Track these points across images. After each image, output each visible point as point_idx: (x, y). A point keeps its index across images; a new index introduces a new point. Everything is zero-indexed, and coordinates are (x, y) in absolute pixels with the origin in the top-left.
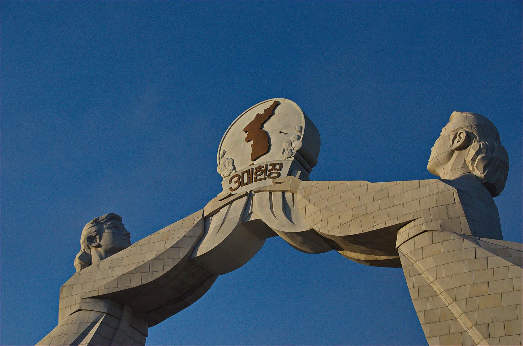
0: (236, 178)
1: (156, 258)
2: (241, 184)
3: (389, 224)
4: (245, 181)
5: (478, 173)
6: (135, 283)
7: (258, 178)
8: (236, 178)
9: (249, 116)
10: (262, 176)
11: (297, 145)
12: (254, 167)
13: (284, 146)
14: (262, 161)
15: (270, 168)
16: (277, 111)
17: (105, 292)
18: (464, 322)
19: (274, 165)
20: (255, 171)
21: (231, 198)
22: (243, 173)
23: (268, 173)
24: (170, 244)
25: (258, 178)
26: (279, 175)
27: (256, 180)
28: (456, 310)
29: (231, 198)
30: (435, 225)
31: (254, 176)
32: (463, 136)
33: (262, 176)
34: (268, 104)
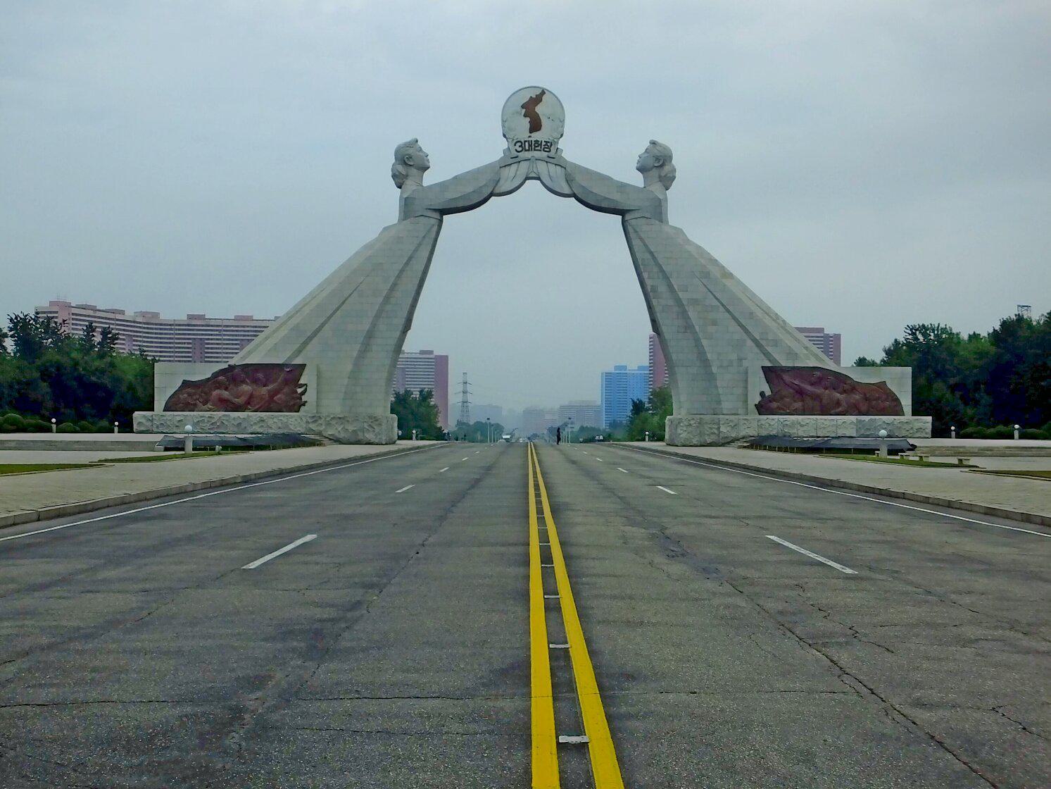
0: (519, 144)
1: (474, 192)
4: (527, 148)
7: (537, 148)
8: (519, 144)
10: (539, 148)
12: (533, 139)
14: (537, 136)
15: (543, 143)
17: (441, 208)
20: (533, 143)
22: (525, 141)
23: (543, 147)
25: (537, 148)
26: (550, 151)
27: (535, 150)
31: (533, 147)
32: (661, 163)
33: (539, 148)
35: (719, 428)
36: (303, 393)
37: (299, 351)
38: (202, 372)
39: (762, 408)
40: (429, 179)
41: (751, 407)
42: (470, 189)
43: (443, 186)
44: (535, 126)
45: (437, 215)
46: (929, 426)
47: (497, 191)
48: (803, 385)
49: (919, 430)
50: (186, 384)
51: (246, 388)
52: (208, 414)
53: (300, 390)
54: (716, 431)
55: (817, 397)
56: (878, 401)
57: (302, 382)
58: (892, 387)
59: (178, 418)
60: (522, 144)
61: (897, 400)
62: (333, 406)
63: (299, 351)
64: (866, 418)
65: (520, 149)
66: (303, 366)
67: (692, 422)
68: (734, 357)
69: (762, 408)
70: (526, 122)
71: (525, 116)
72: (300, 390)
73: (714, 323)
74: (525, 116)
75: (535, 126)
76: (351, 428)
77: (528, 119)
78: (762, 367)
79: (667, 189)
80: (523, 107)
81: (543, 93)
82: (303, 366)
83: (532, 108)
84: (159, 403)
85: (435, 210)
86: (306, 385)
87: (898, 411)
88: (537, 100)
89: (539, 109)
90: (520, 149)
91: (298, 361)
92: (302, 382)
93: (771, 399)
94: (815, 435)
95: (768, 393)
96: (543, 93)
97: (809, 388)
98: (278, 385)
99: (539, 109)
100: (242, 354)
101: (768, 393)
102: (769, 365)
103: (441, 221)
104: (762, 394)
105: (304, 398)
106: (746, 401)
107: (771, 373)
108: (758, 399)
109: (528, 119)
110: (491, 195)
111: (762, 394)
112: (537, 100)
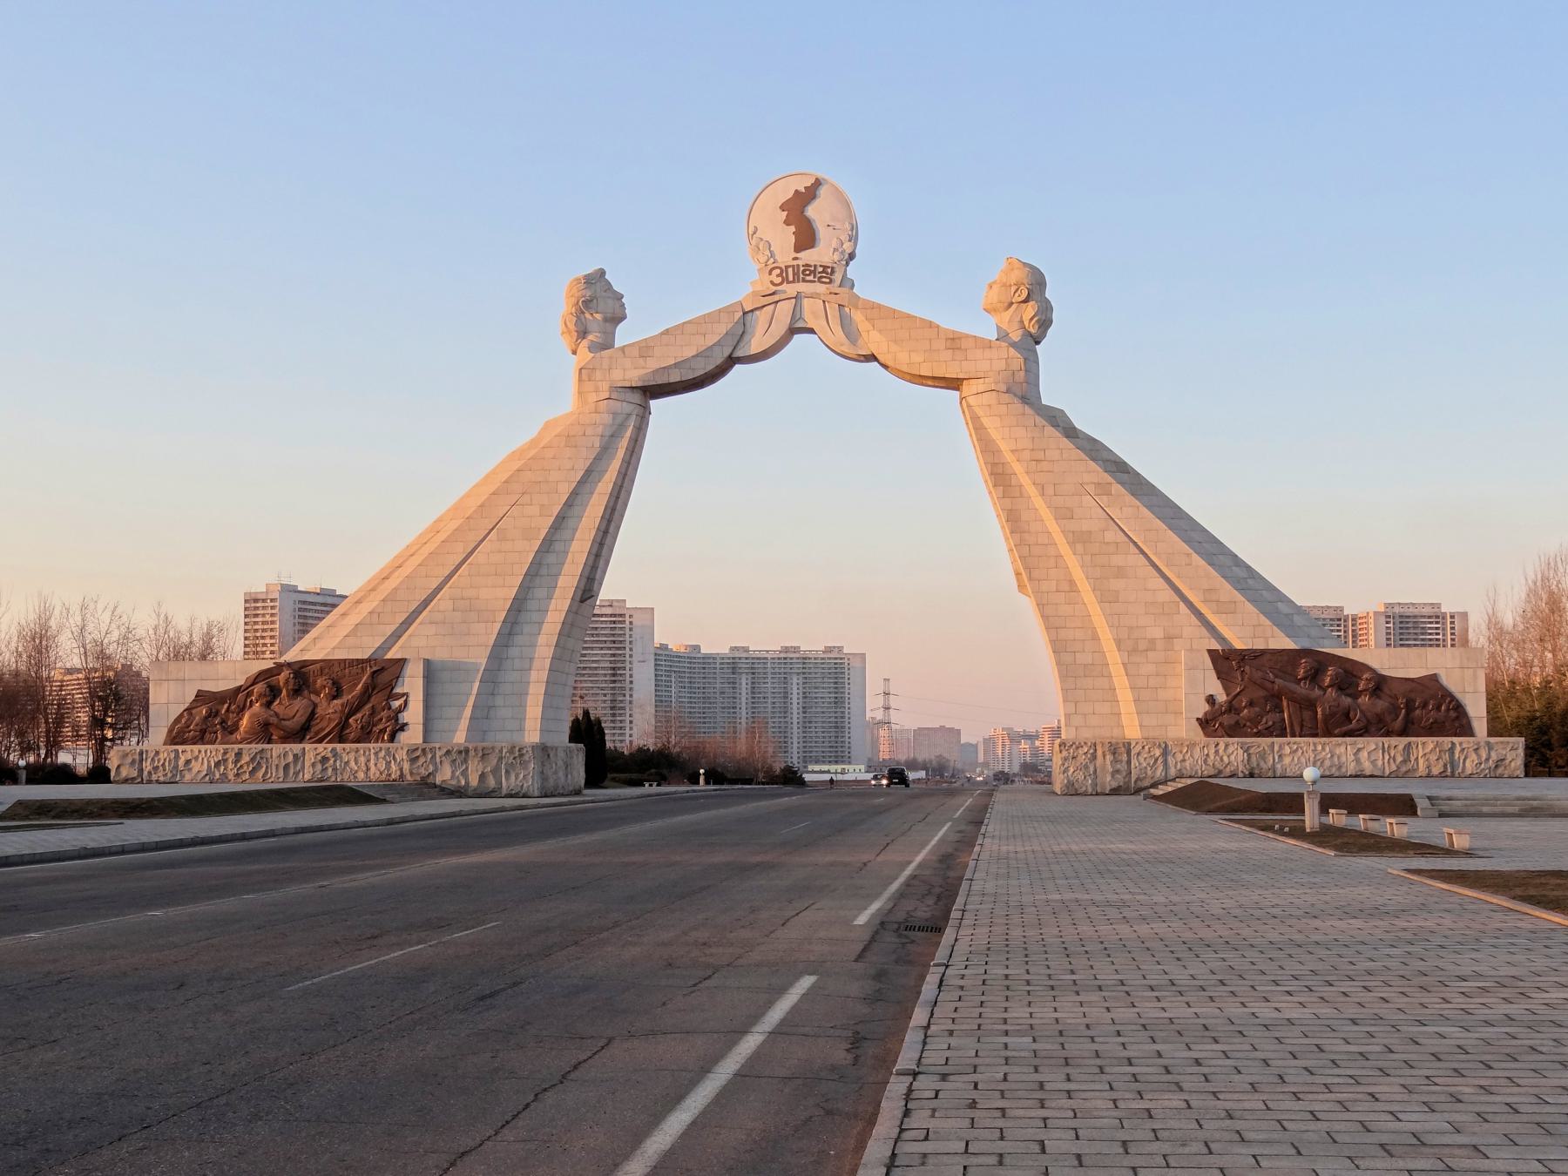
2: (785, 280)
3: (961, 376)
5: (1033, 331)
6: (675, 377)
11: (848, 247)
12: (800, 263)
13: (835, 243)
14: (808, 257)
16: (823, 191)
18: (1025, 480)
19: (825, 267)
21: (776, 298)
24: (712, 340)
28: (1018, 468)
29: (776, 298)
30: (1004, 388)
35: (1129, 762)
37: (397, 635)
39: (1215, 722)
40: (624, 335)
42: (690, 352)
43: (644, 349)
44: (806, 237)
45: (637, 398)
46: (1521, 751)
47: (739, 353)
48: (1291, 685)
49: (1500, 762)
50: (201, 697)
53: (396, 704)
55: (1311, 705)
56: (1425, 710)
57: (398, 690)
58: (1450, 682)
60: (783, 273)
61: (1459, 708)
63: (397, 635)
66: (401, 663)
68: (1157, 633)
70: (788, 235)
71: (787, 222)
72: (396, 704)
73: (1120, 572)
74: (787, 222)
75: (806, 237)
77: (793, 229)
78: (1210, 651)
79: (1038, 343)
80: (782, 208)
81: (818, 183)
82: (401, 663)
83: (797, 209)
84: (157, 735)
85: (632, 388)
86: (406, 694)
87: (1465, 729)
88: (809, 195)
89: (811, 211)
91: (389, 656)
92: (398, 690)
93: (1231, 708)
95: (1222, 697)
96: (818, 183)
97: (1293, 686)
98: (361, 696)
99: (811, 211)
100: (301, 645)
101: (1222, 697)
102: (1216, 646)
103: (645, 412)
104: (1211, 700)
105: (405, 717)
107: (1227, 662)
109: (793, 229)
110: (731, 361)
111: (1211, 700)
112: (809, 195)
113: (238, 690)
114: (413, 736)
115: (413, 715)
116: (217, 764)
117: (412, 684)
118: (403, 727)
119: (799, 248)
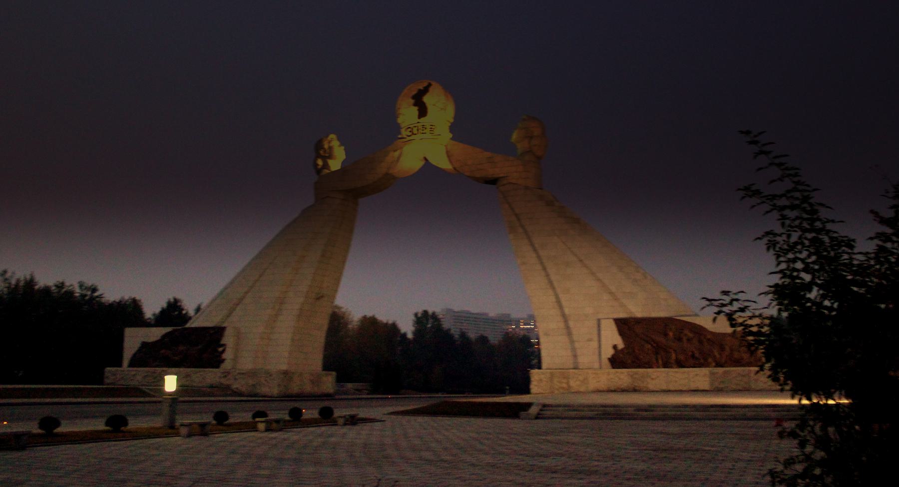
9: (414, 88)
16: (431, 89)
34: (426, 84)
36: (223, 351)
38: (155, 334)
39: (616, 362)
41: (605, 362)
50: (144, 345)
51: (181, 348)
52: (152, 369)
54: (565, 385)
57: (222, 342)
59: (133, 373)
62: (247, 363)
64: (720, 370)
65: (410, 134)
67: (542, 376)
69: (616, 362)
71: (415, 105)
72: (221, 349)
76: (251, 382)
81: (430, 85)
86: (224, 345)
89: (426, 99)
90: (410, 134)
91: (224, 325)
92: (222, 342)
94: (664, 388)
95: (621, 345)
102: (622, 315)
105: (224, 356)
106: (600, 355)
107: (624, 325)
108: (610, 352)
111: (615, 347)
112: (425, 91)
113: (157, 342)
114: (227, 365)
115: (228, 355)
116: (145, 377)
117: (228, 339)
118: (223, 361)
119: (420, 116)
